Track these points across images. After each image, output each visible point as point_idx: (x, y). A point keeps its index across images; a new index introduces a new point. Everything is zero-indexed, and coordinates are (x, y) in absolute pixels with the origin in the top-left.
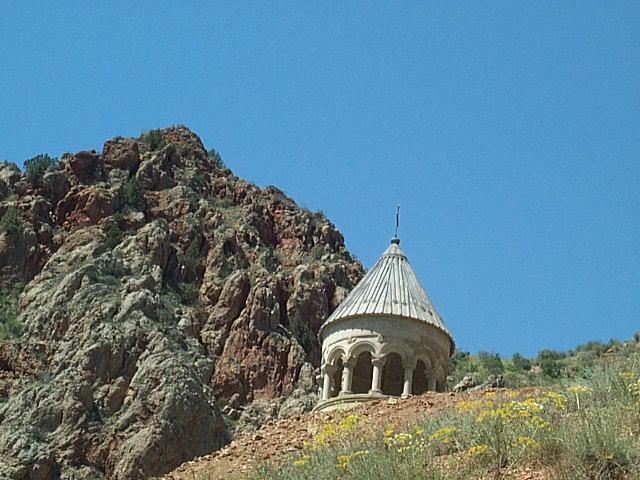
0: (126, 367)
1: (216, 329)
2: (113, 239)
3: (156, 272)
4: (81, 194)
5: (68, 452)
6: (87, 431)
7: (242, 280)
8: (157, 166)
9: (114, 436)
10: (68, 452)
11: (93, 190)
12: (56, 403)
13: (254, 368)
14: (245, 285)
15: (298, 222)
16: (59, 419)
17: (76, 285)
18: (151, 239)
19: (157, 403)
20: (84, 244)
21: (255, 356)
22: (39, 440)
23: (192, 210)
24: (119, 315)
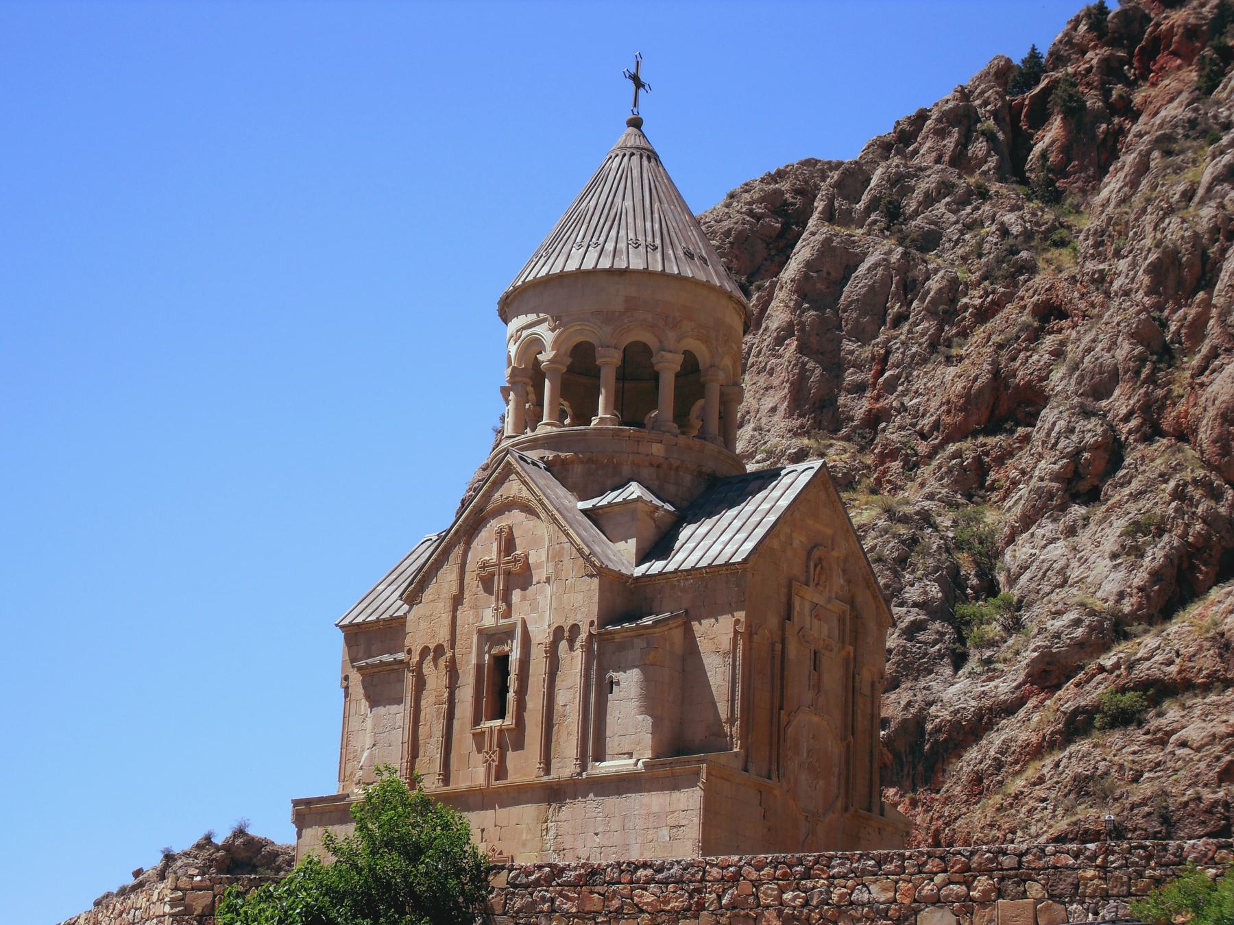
4: (1163, 27)
5: (1133, 423)
6: (1157, 386)
9: (1190, 385)
10: (1133, 423)
12: (1108, 355)
16: (1114, 377)
17: (1142, 167)
20: (1171, 100)
22: (1087, 414)
24: (1196, 199)
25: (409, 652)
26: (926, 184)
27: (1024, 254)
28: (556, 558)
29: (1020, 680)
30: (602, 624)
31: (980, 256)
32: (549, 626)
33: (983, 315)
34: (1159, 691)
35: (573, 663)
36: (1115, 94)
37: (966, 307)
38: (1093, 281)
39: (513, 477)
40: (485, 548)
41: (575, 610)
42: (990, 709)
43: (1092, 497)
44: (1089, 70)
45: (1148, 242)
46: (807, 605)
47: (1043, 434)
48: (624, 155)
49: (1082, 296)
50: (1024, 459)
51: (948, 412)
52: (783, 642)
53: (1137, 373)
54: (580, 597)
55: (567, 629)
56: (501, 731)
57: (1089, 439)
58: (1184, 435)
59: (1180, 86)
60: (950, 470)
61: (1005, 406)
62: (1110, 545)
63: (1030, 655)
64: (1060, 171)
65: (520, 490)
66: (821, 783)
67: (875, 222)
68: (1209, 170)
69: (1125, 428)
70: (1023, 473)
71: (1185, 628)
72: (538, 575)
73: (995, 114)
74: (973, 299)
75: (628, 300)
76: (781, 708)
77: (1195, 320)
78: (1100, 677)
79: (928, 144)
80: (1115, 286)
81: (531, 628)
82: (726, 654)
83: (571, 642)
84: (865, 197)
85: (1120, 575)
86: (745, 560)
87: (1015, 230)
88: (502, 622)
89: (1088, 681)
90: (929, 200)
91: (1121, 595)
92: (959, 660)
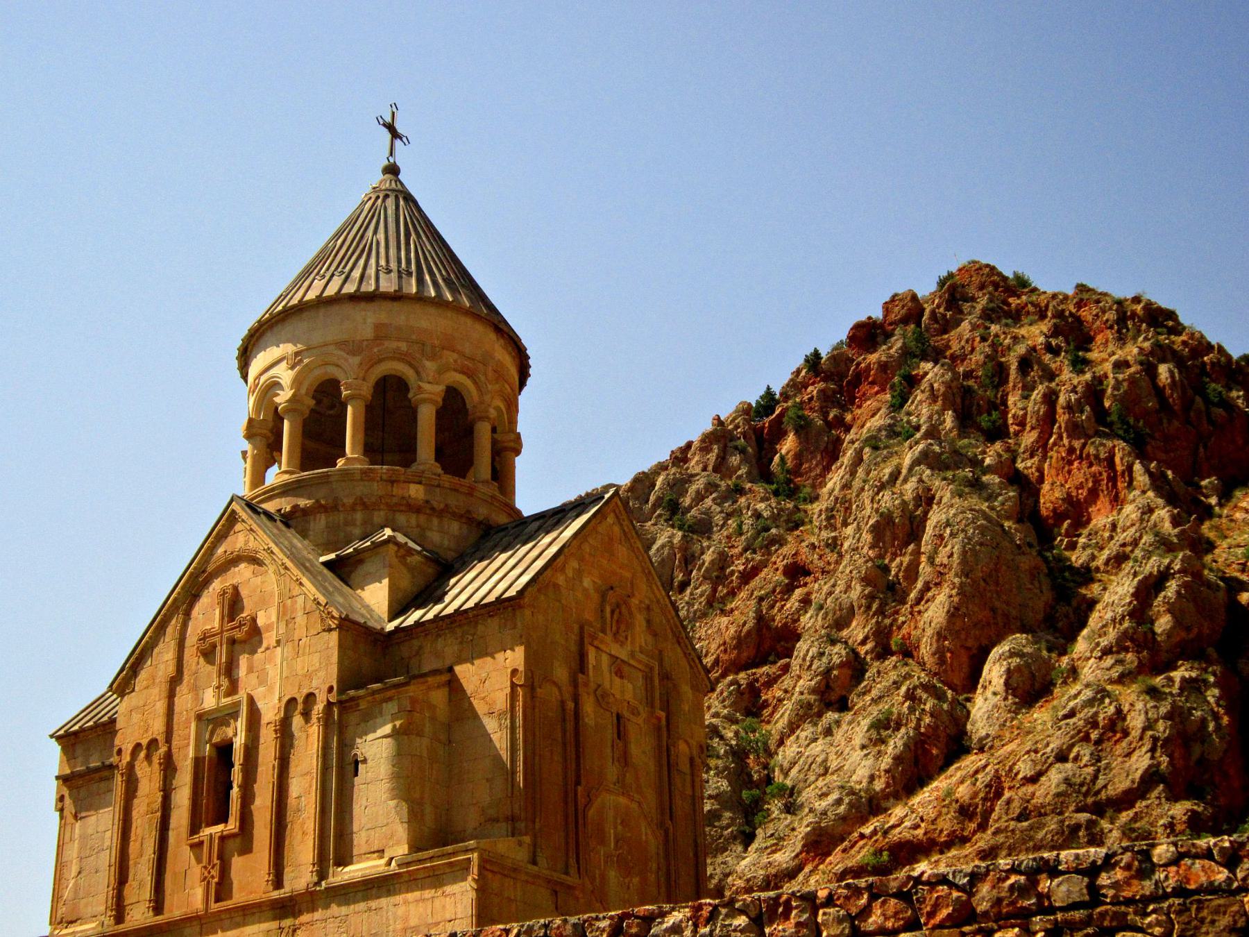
0: (914, 531)
1: (1032, 456)
2: (902, 399)
3: (949, 419)
5: (869, 646)
6: (885, 617)
7: (1045, 396)
8: (942, 310)
9: (911, 613)
10: (869, 646)
11: (873, 358)
12: (844, 596)
13: (1081, 486)
14: (1050, 399)
15: (1104, 312)
16: (851, 612)
17: (858, 460)
18: (936, 386)
19: (945, 561)
20: (873, 416)
21: (1080, 474)
22: (833, 642)
23: (984, 339)
24: (901, 478)
25: (120, 752)
26: (699, 484)
27: (774, 531)
28: (285, 614)
29: (798, 850)
30: (342, 690)
31: (741, 534)
32: (280, 699)
33: (747, 577)
34: (907, 852)
35: (309, 741)
36: (831, 415)
37: (732, 573)
38: (828, 545)
39: (238, 527)
40: (207, 614)
41: (309, 676)
42: (775, 876)
43: (843, 705)
44: (811, 399)
45: (868, 511)
46: (605, 659)
47: (800, 661)
48: (378, 197)
49: (821, 557)
50: (787, 682)
51: (725, 651)
52: (576, 699)
53: (869, 607)
54: (316, 659)
55: (300, 700)
56: (223, 838)
57: (836, 660)
58: (908, 652)
59: (878, 405)
60: (731, 693)
61: (770, 643)
62: (858, 740)
63: (803, 830)
64: (796, 471)
65: (247, 542)
66: (636, 880)
67: (660, 516)
68: (909, 455)
69: (862, 650)
70: (786, 691)
71: (925, 798)
72: (269, 639)
73: (744, 434)
74: (738, 566)
75: (378, 327)
76: (578, 783)
77: (910, 564)
78: (861, 843)
79: (697, 458)
80: (846, 545)
81: (260, 705)
82: (501, 714)
83: (306, 715)
84: (652, 498)
85: (869, 762)
86: (521, 593)
87: (765, 514)
88: (226, 701)
89: (852, 847)
90: (699, 497)
91: (872, 778)
92: (747, 839)
